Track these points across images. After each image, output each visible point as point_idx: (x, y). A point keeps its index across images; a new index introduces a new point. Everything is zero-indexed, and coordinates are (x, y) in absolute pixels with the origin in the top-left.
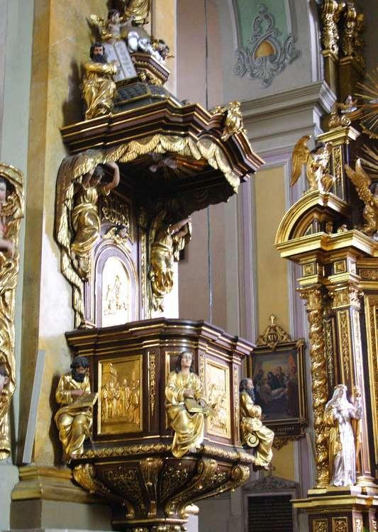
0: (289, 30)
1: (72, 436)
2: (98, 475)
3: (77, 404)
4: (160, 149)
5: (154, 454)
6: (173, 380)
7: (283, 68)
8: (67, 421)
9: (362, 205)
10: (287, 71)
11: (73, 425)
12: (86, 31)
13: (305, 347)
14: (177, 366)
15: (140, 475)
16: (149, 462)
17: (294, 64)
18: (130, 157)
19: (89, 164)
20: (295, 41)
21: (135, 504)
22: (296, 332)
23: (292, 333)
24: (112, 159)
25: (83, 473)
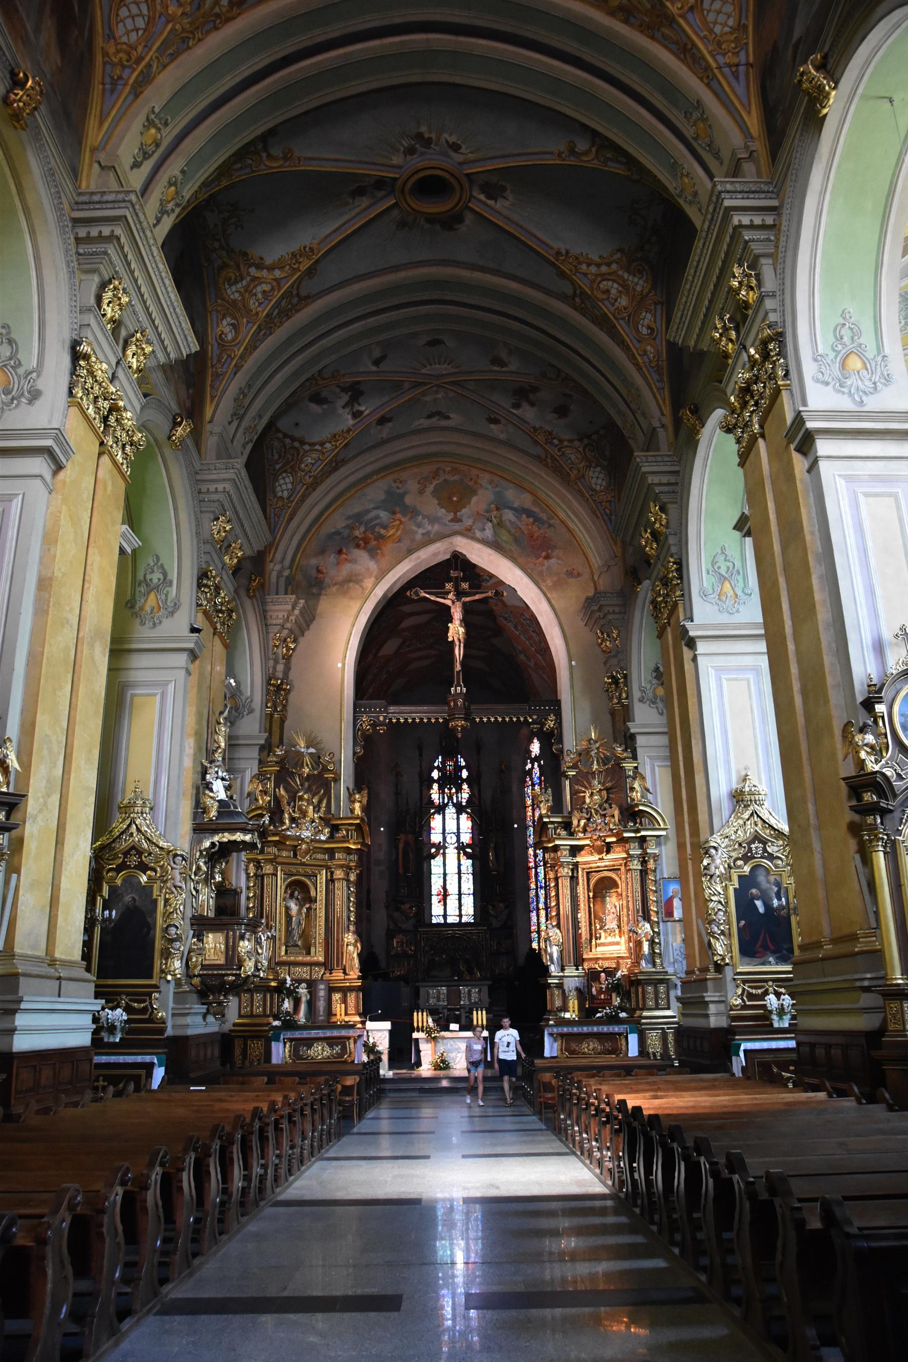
0: (249, 694)
1: (195, 967)
2: (202, 983)
3: (199, 952)
4: (239, 840)
5: (233, 975)
6: (241, 943)
7: (243, 717)
8: (194, 960)
9: (282, 812)
10: (246, 717)
11: (197, 961)
12: (199, 769)
13: (241, 892)
14: (242, 937)
15: (225, 983)
16: (230, 978)
17: (250, 716)
18: (225, 840)
19: (207, 844)
20: (252, 701)
21: (213, 994)
22: (237, 883)
23: (234, 883)
24: (216, 838)
25: (196, 981)
